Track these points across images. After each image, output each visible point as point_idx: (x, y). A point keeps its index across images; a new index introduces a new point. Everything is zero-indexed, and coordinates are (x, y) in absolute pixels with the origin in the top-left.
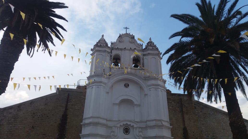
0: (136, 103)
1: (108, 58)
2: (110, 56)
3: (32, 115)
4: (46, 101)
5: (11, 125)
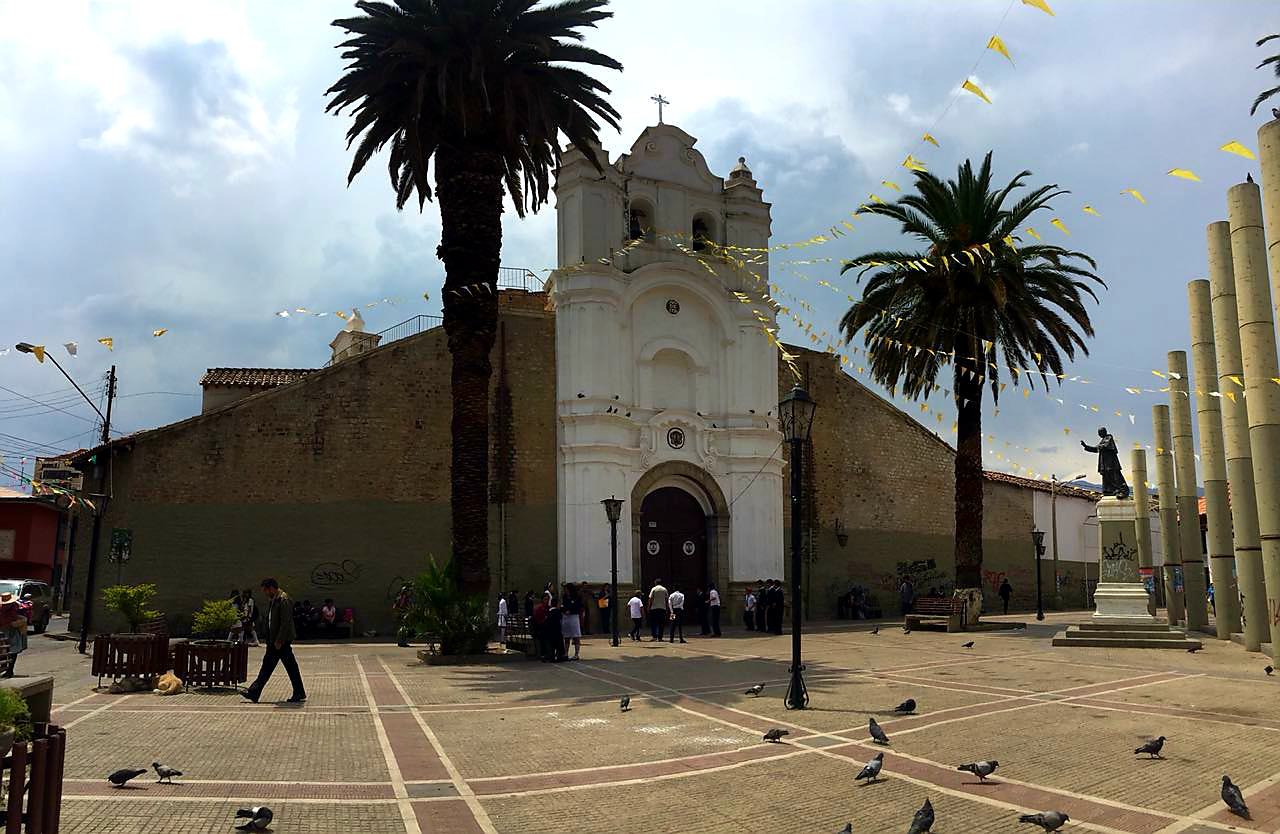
0: (698, 361)
1: (619, 210)
2: (622, 204)
3: (406, 391)
4: (437, 345)
5: (352, 420)
